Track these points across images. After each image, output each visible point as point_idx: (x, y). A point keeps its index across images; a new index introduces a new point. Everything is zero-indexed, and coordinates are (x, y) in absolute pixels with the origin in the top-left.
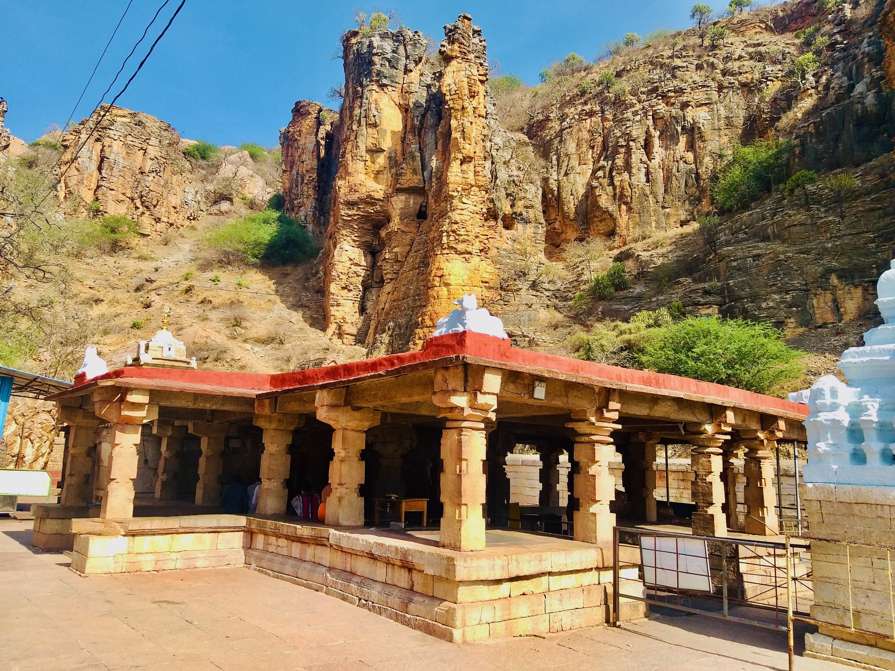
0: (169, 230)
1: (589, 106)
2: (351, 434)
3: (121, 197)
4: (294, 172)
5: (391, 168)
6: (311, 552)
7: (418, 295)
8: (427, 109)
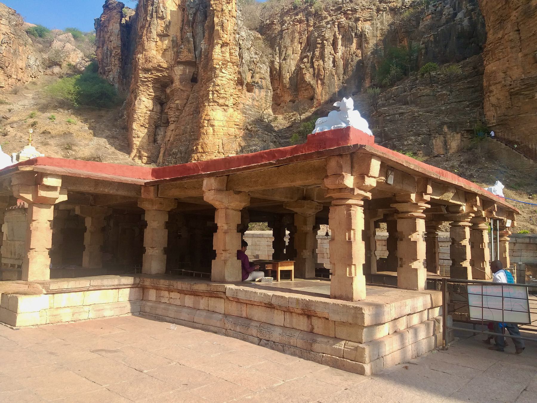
1: (299, 17)
2: (231, 212)
4: (105, 48)
5: (173, 48)
6: (203, 302)
7: (193, 132)
8: (197, 10)
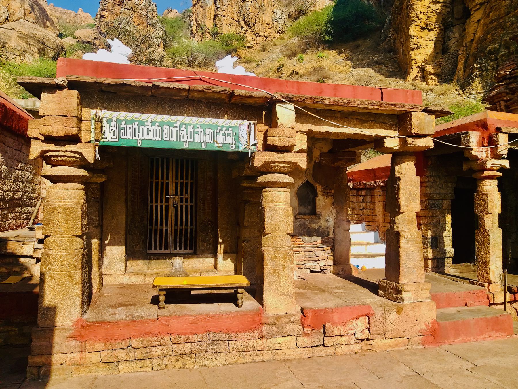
0: (266, 42)
3: (231, 21)
